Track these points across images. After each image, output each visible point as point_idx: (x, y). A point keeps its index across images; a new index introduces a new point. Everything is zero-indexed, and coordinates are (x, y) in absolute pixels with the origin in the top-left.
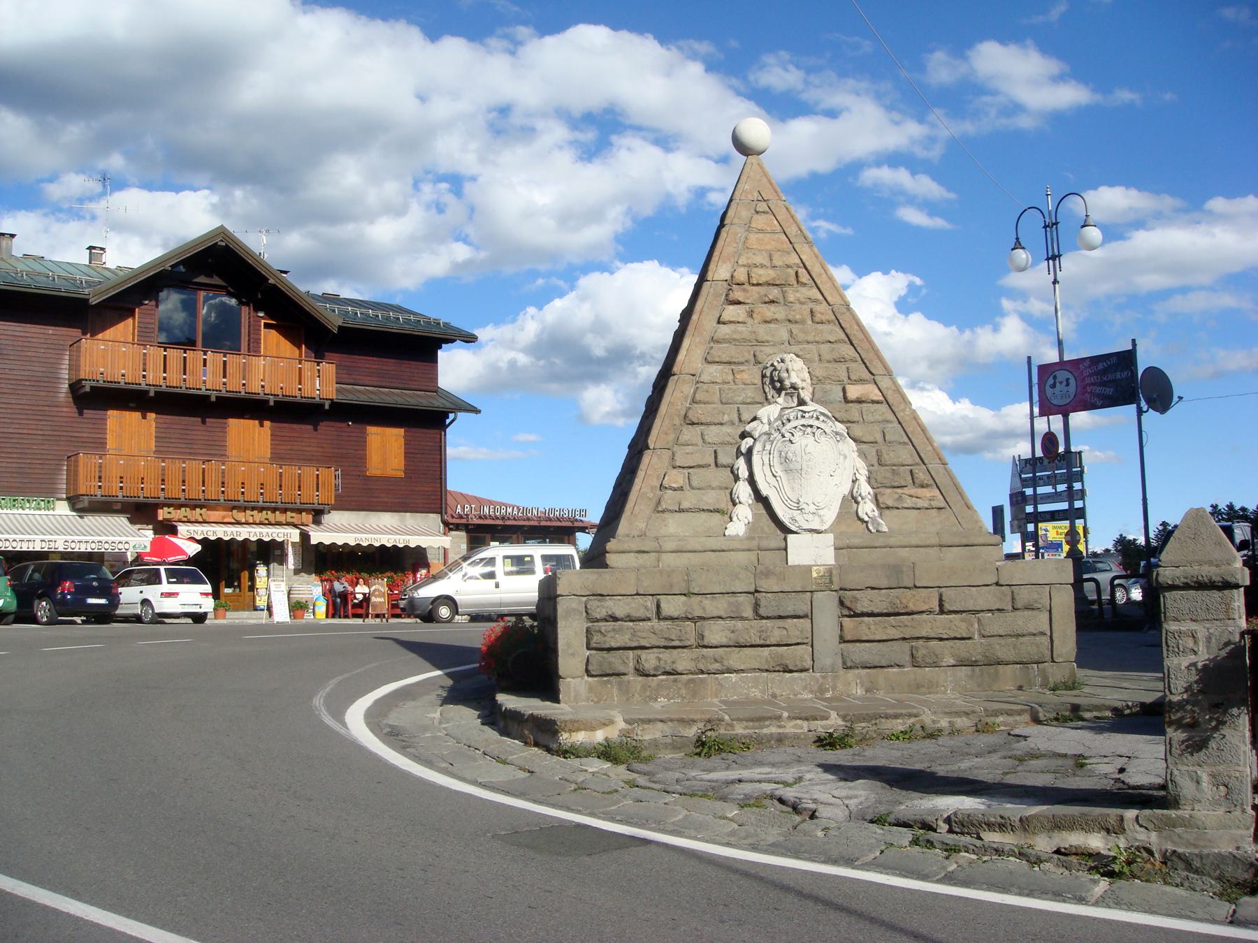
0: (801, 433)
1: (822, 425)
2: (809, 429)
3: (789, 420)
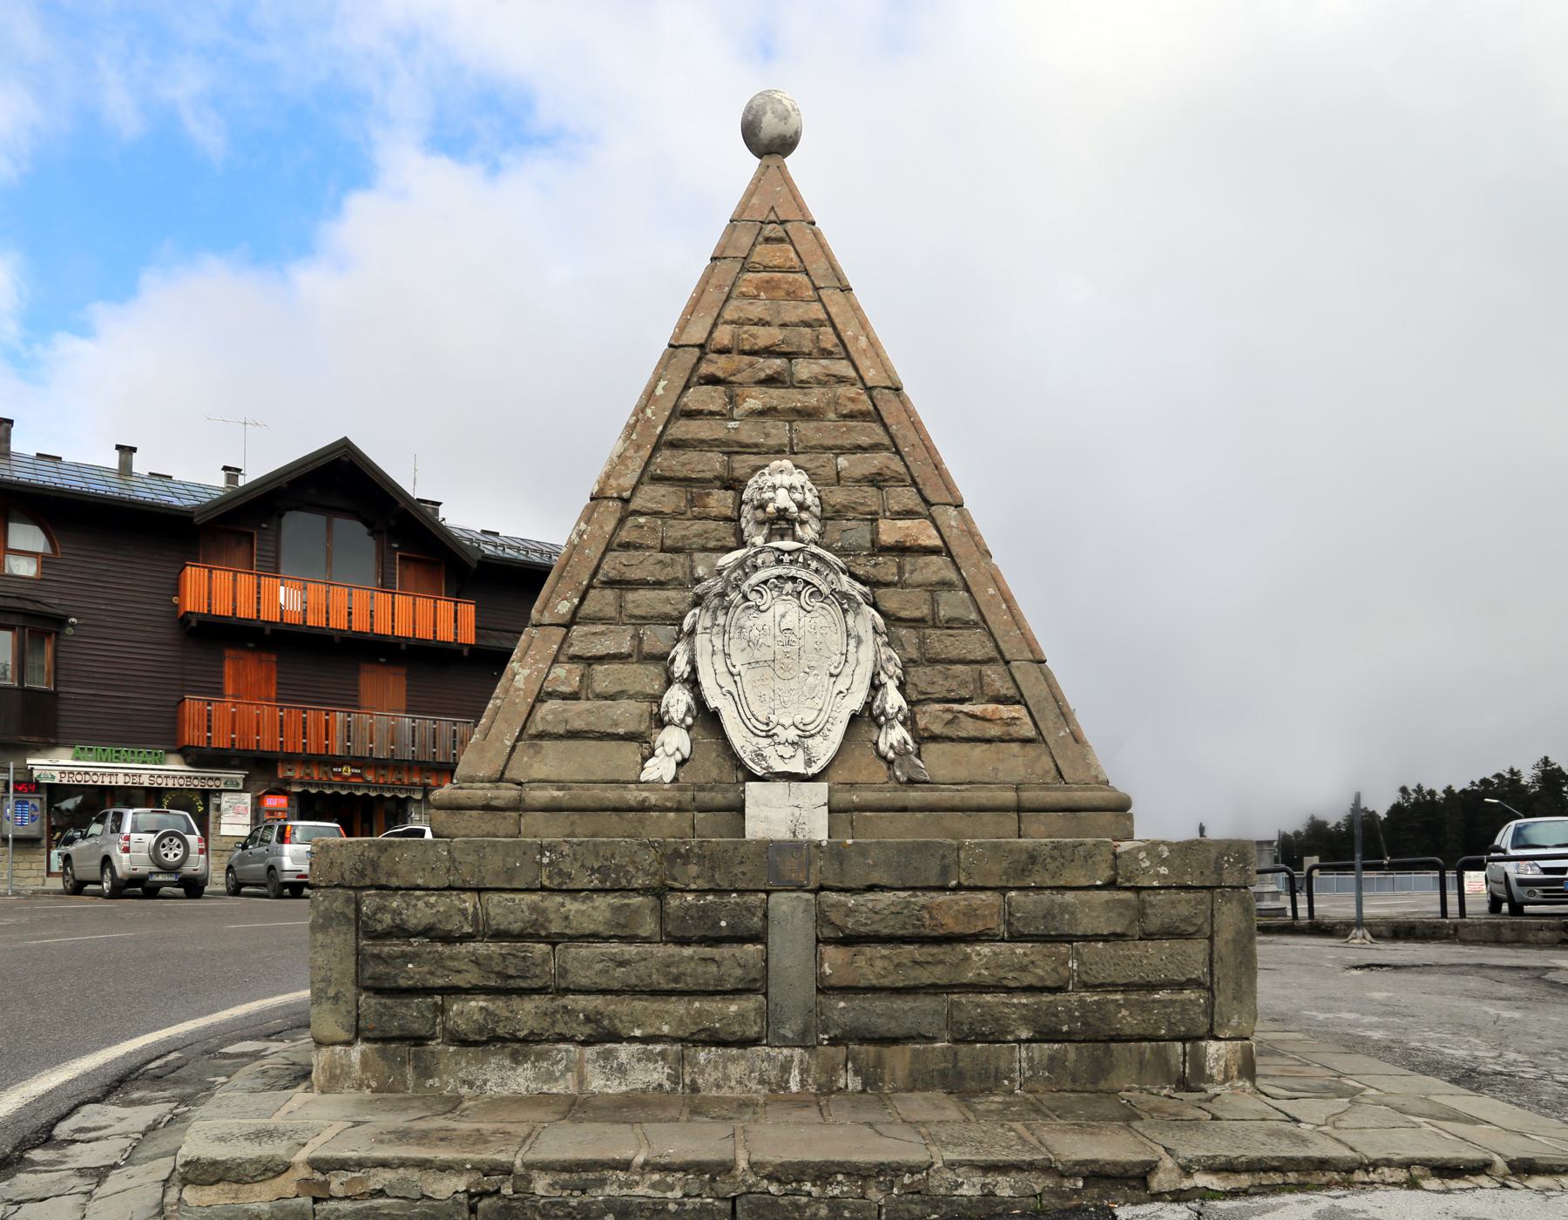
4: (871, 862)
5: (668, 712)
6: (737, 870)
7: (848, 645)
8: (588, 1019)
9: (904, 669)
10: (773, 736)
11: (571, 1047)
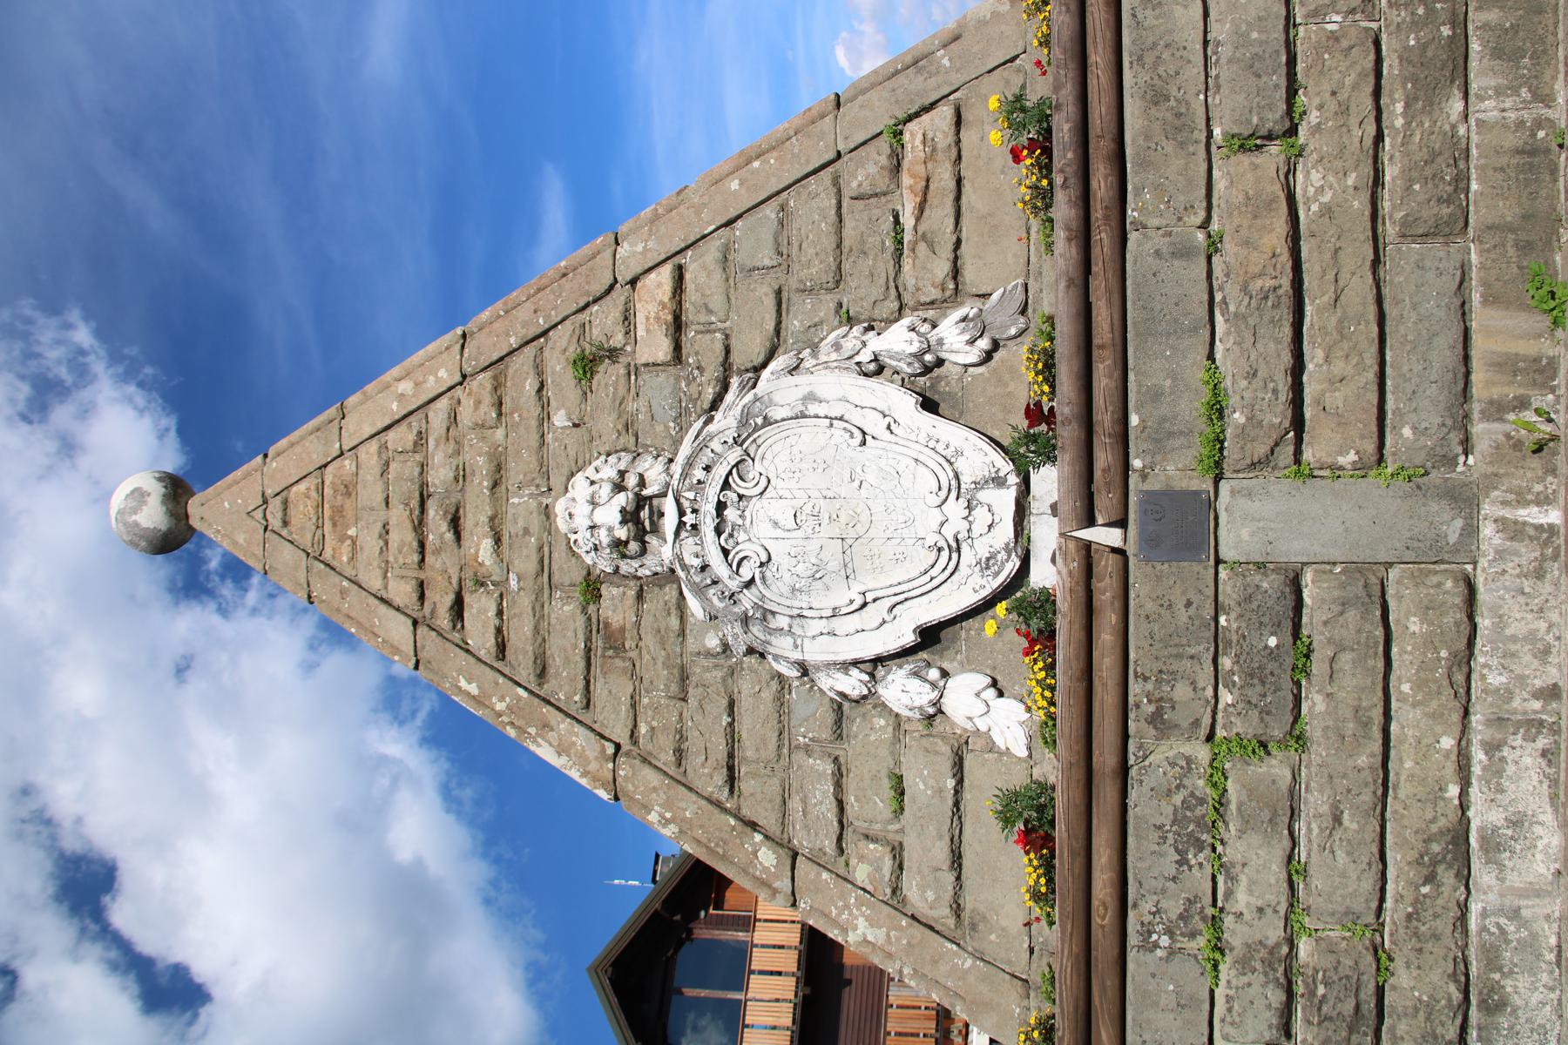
0: (742, 537)
1: (720, 471)
2: (731, 514)
3: (704, 568)
4: (1168, 382)
5: (921, 708)
6: (1183, 616)
7: (817, 417)
8: (1430, 878)
9: (850, 321)
10: (957, 541)
11: (1475, 908)
